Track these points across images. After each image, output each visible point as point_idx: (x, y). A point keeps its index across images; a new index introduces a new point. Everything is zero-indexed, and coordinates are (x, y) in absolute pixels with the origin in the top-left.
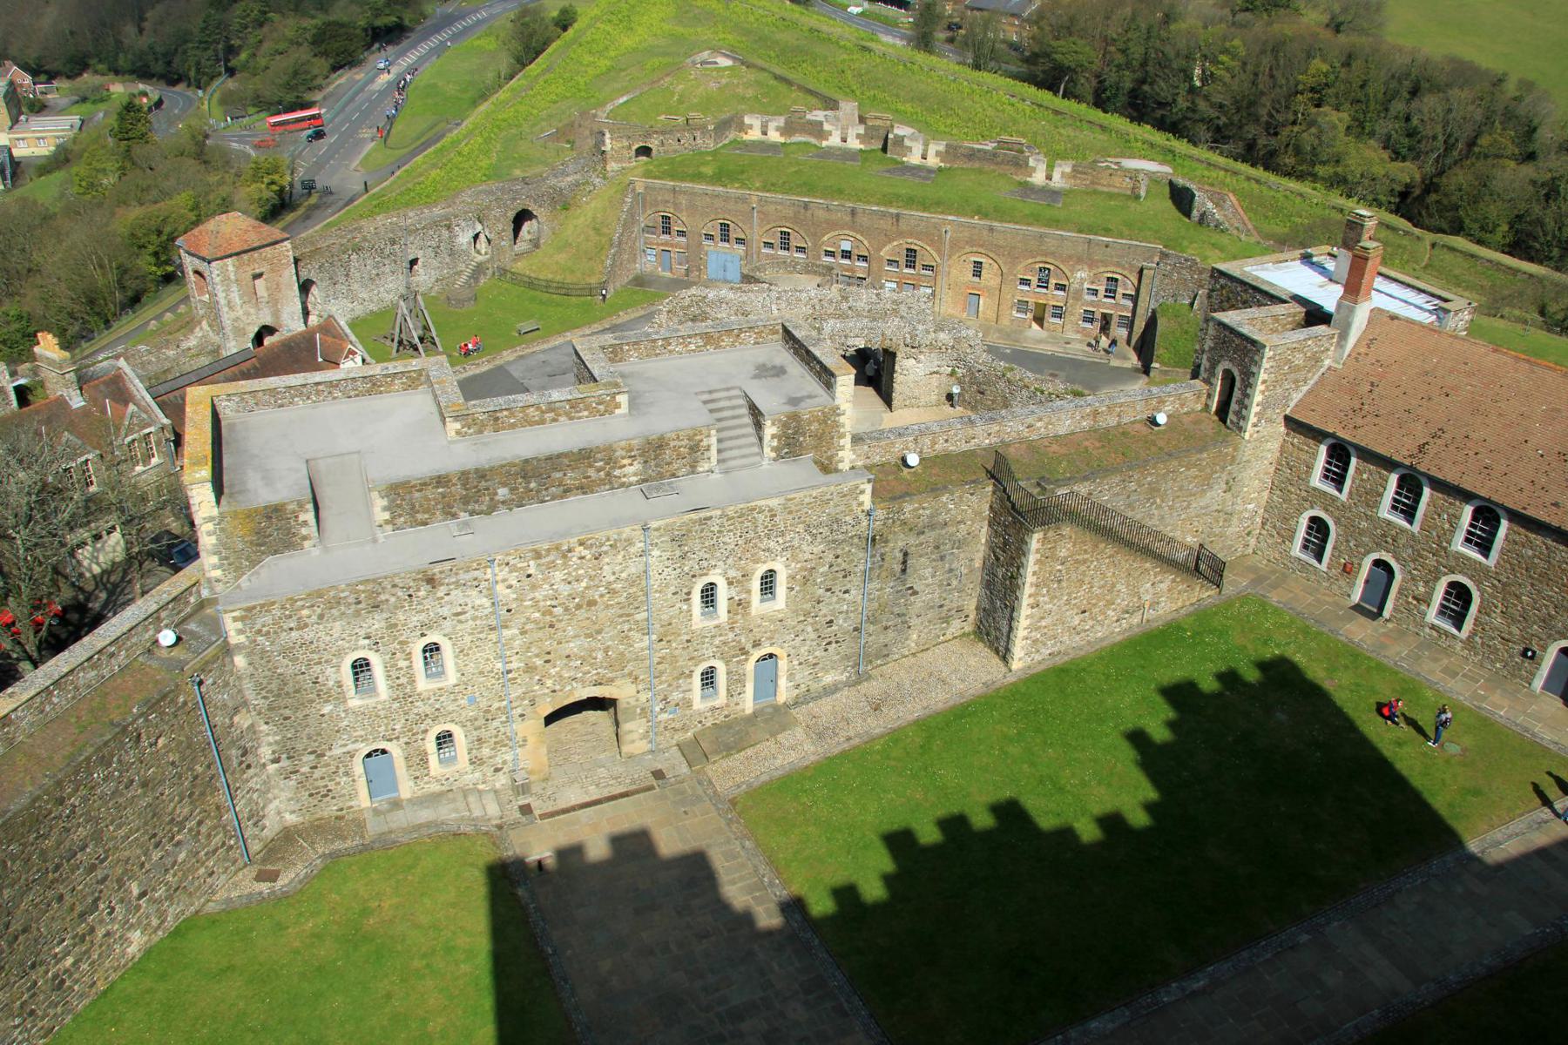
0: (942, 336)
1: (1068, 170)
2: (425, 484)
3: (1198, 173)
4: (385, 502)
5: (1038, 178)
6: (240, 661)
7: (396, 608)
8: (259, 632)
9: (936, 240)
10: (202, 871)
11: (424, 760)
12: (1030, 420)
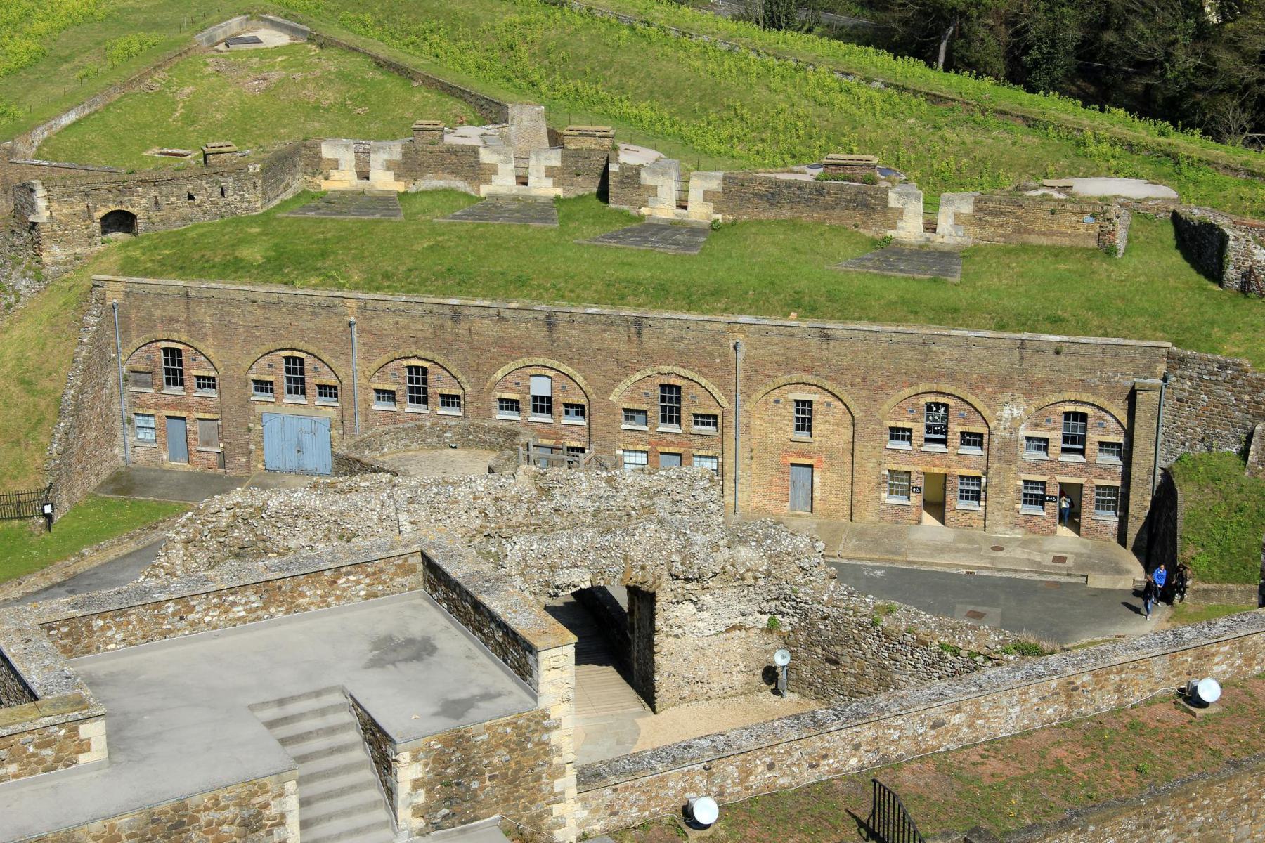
0: (745, 553)
1: (967, 208)
3: (1230, 192)
5: (910, 230)
12: (937, 712)
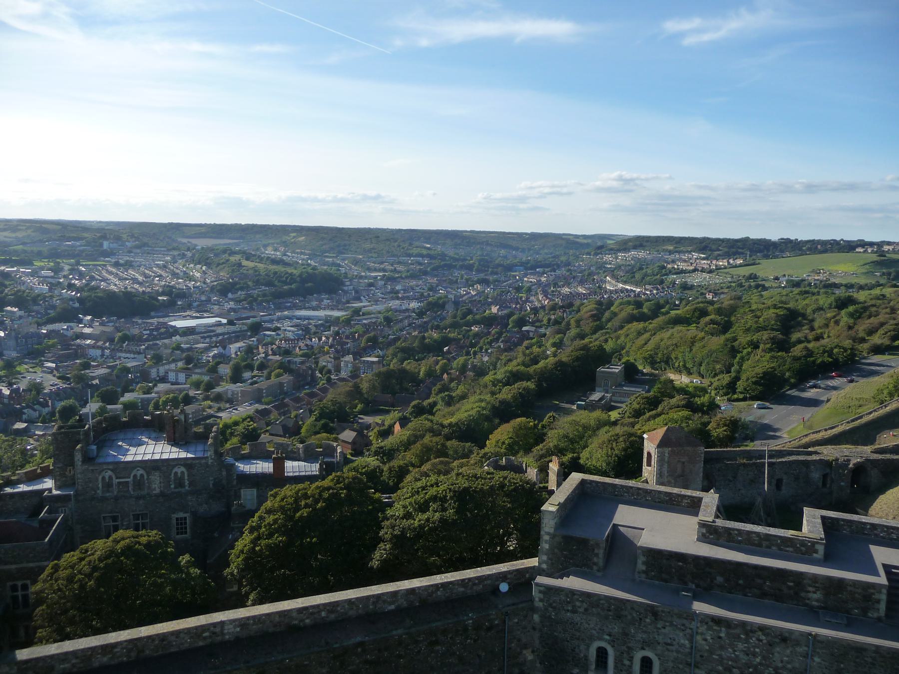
8: (550, 605)
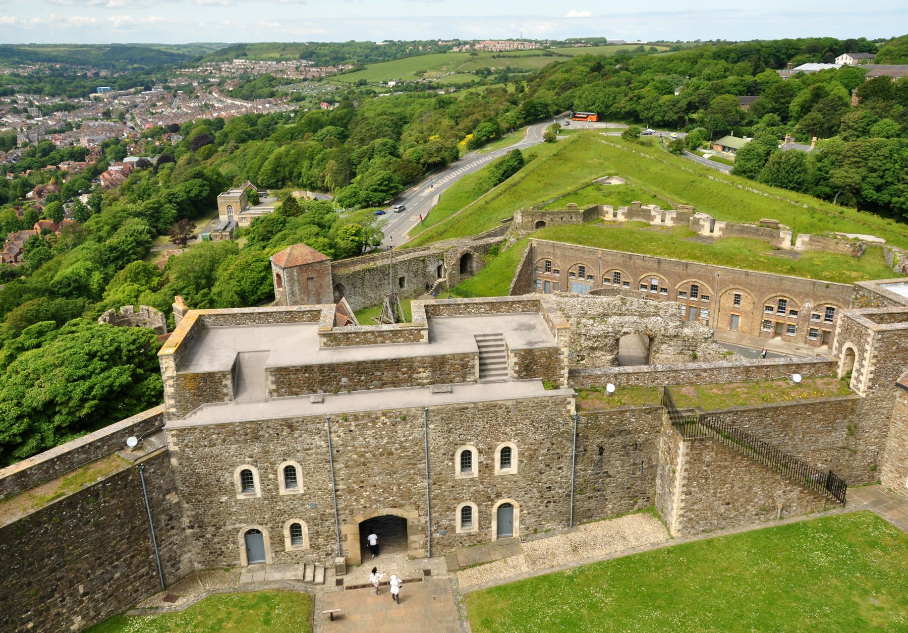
2: (298, 370)
4: (273, 379)
6: (174, 461)
7: (269, 441)
8: (187, 445)
9: (710, 281)
10: (130, 587)
11: (282, 542)
